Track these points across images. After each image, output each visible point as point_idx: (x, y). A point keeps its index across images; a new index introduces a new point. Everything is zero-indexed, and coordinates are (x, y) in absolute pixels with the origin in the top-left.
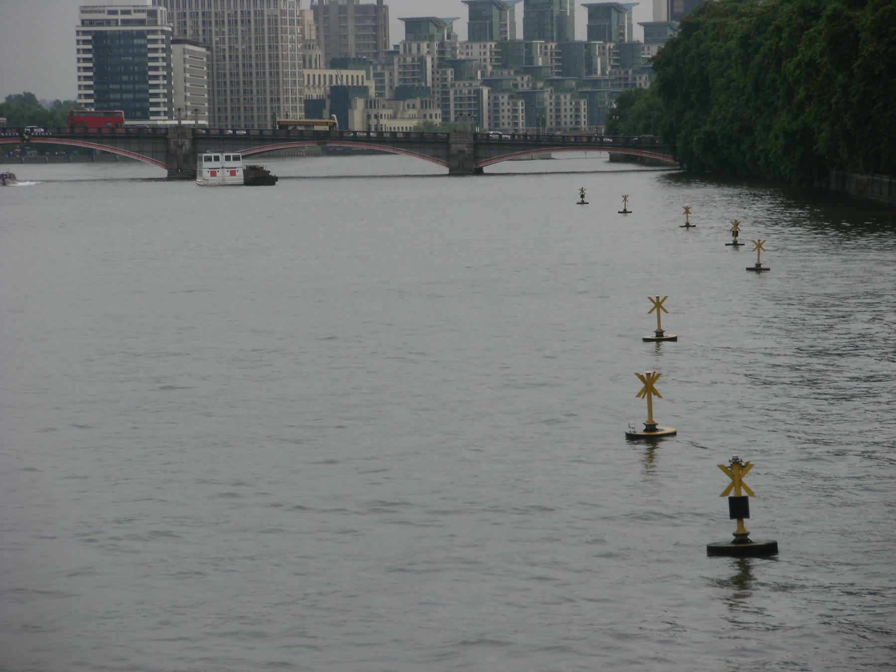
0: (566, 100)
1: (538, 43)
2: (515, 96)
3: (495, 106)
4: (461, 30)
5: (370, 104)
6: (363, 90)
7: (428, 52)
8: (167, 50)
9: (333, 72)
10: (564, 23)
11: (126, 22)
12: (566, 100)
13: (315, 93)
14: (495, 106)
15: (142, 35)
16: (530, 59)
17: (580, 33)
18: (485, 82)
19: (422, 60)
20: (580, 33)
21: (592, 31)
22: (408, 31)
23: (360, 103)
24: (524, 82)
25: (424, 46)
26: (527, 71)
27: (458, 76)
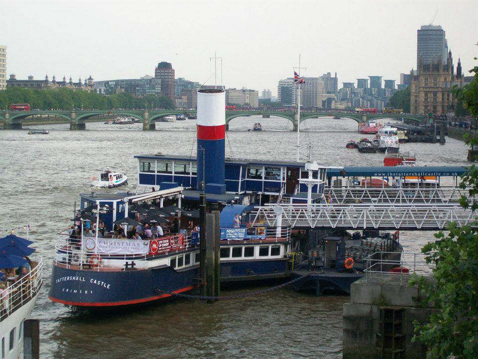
0: (379, 102)
1: (373, 89)
2: (368, 100)
3: (363, 103)
4: (356, 86)
5: (336, 102)
6: (334, 99)
7: (348, 90)
8: (296, 91)
9: (328, 95)
10: (380, 85)
11: (288, 85)
12: (379, 102)
13: (324, 99)
14: (363, 103)
15: (291, 87)
16: (371, 92)
17: (383, 86)
18: (362, 97)
19: (347, 92)
20: (383, 86)
21: (386, 86)
22: (344, 86)
23: (334, 101)
24: (370, 97)
25: (348, 89)
26: (370, 95)
27: (355, 96)
